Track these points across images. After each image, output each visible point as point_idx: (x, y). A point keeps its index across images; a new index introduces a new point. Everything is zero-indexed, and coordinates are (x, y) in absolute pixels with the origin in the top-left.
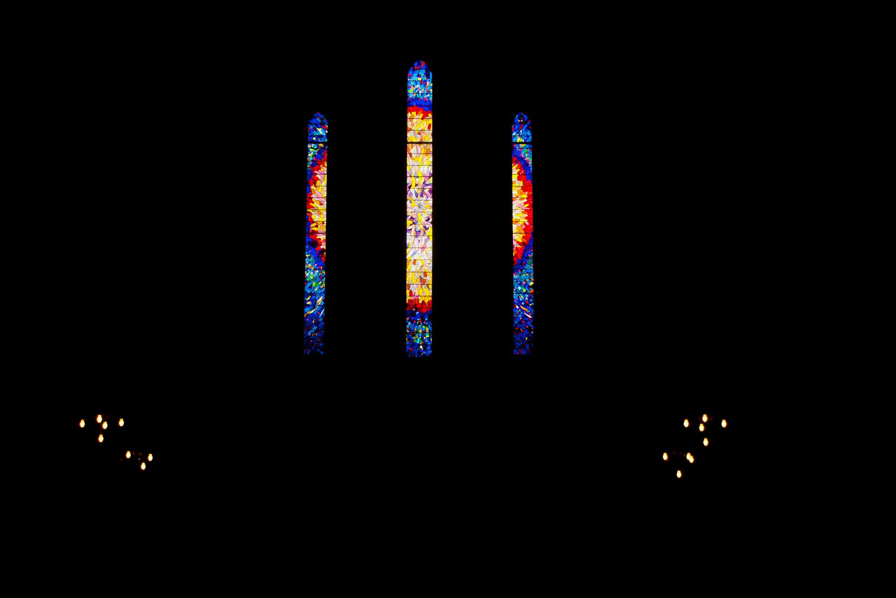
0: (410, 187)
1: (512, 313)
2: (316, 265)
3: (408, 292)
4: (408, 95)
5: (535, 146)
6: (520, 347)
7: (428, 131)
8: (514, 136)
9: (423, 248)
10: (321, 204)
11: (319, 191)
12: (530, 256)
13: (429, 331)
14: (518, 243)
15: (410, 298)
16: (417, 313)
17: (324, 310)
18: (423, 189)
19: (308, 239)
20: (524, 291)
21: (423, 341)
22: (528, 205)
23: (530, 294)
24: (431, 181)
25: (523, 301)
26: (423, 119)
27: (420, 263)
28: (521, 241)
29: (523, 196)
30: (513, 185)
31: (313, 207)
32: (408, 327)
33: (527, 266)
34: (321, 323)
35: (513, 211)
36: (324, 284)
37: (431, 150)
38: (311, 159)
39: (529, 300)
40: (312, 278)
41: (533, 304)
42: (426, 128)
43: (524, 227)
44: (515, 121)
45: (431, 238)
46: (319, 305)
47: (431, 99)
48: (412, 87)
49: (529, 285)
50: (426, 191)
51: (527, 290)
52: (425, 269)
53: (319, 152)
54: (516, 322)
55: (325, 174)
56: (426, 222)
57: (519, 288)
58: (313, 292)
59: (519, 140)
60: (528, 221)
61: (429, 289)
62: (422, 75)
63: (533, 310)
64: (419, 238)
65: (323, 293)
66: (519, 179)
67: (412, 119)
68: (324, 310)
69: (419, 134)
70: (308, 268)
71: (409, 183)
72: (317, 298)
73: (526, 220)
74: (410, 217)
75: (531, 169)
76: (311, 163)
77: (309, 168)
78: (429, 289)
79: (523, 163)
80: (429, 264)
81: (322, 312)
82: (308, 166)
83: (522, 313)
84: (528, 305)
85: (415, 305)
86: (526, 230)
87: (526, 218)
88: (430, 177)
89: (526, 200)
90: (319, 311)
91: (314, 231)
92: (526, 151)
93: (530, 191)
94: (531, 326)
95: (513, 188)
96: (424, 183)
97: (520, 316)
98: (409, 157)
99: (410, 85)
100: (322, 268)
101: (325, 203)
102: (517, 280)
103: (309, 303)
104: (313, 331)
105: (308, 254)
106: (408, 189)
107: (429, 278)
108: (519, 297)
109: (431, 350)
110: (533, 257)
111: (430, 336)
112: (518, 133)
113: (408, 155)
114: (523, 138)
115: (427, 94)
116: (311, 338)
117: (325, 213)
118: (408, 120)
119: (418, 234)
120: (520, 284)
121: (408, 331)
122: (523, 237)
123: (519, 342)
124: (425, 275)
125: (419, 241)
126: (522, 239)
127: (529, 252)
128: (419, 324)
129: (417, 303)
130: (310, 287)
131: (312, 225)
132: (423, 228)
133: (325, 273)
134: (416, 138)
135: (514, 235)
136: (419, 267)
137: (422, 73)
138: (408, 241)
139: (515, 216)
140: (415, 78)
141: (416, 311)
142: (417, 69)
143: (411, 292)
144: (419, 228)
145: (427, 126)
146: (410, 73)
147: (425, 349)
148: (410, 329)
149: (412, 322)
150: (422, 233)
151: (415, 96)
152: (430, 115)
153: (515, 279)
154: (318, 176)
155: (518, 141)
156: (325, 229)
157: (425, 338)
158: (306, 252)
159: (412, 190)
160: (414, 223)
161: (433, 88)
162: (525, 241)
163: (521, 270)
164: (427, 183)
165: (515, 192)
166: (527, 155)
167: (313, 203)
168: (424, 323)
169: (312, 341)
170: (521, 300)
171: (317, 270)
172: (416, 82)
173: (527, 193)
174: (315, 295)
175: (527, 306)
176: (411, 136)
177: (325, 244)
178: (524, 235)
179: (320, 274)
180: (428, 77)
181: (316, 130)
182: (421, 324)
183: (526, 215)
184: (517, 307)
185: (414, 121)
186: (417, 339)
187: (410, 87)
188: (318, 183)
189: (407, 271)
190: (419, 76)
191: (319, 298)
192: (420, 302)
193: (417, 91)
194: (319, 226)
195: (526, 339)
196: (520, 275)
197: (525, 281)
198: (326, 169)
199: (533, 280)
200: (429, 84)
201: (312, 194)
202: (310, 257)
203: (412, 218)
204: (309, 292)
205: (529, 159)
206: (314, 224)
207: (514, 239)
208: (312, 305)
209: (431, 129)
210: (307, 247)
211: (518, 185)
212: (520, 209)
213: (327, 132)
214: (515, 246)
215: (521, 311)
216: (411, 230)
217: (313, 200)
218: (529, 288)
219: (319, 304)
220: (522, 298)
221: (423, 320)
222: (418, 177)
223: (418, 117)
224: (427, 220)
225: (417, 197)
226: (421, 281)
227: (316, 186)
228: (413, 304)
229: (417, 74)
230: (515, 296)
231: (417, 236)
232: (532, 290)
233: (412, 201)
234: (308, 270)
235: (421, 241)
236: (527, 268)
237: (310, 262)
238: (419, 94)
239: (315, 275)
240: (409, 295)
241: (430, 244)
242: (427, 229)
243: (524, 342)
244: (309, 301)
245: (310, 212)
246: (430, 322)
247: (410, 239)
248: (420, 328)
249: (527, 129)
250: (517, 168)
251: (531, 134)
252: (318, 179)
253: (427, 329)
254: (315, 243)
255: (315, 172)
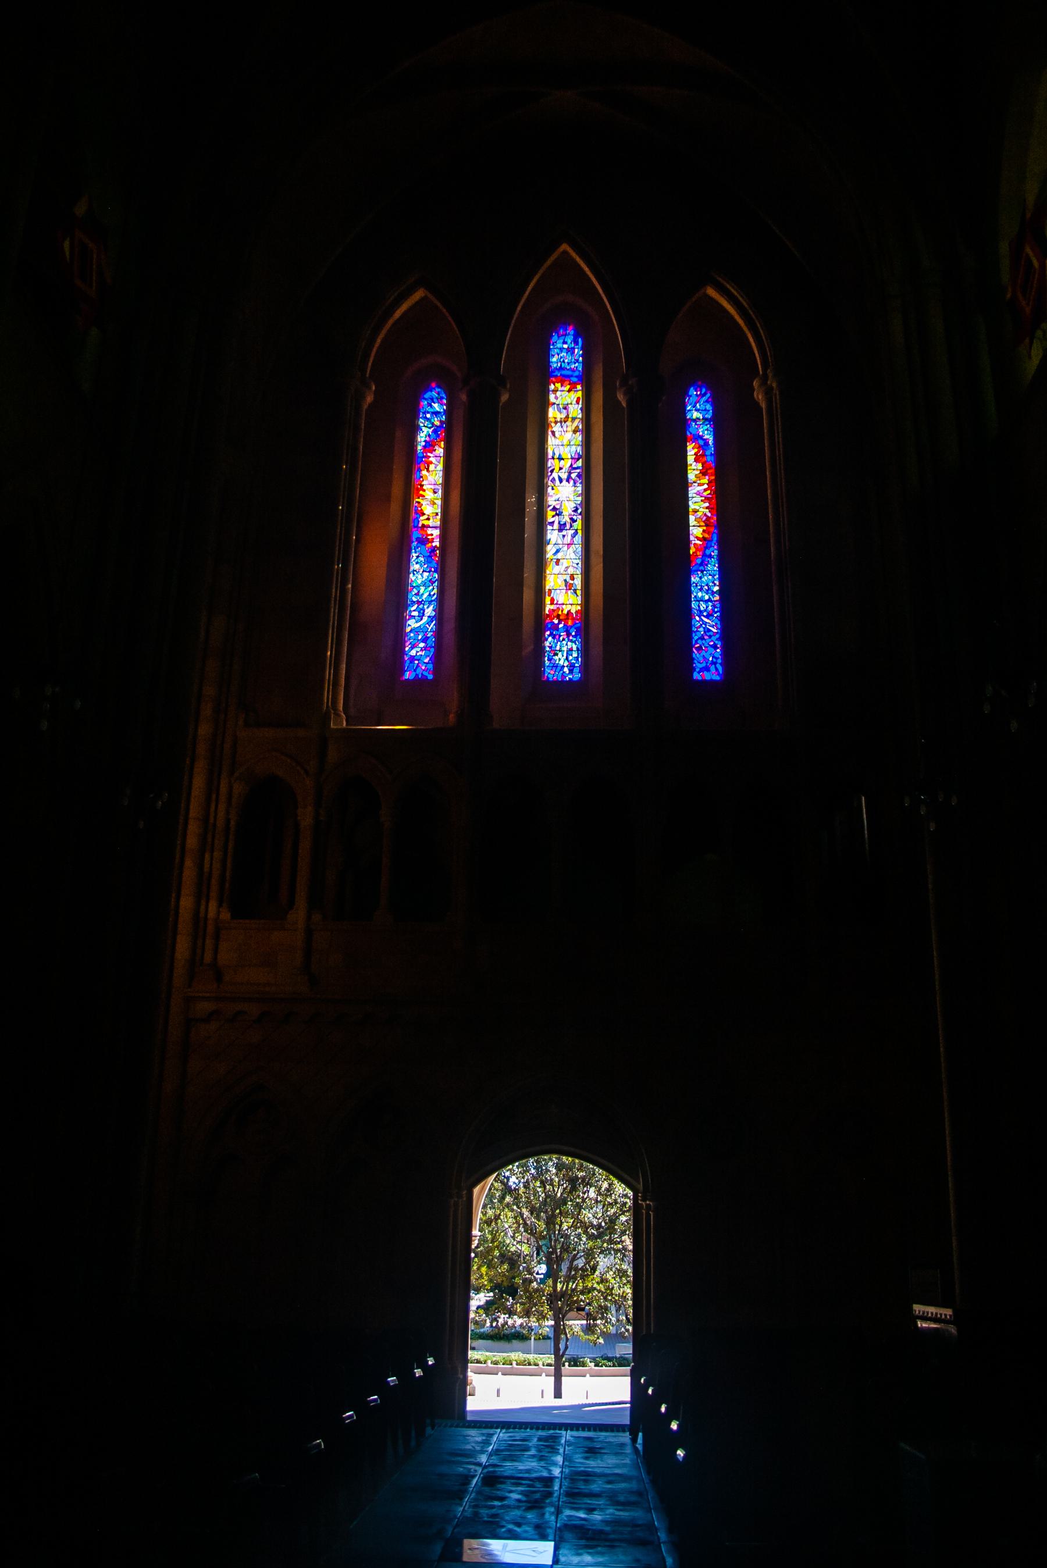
0: (552, 471)
1: (691, 626)
2: (426, 566)
3: (548, 600)
4: (551, 364)
5: (716, 422)
6: (702, 670)
7: (577, 405)
8: (689, 410)
9: (569, 545)
10: (435, 492)
11: (432, 476)
12: (713, 554)
13: (578, 649)
14: (698, 538)
15: (552, 607)
16: (561, 626)
17: (434, 622)
18: (570, 473)
19: (416, 535)
20: (707, 597)
21: (568, 661)
22: (709, 492)
23: (714, 601)
24: (579, 463)
25: (705, 610)
26: (569, 391)
27: (564, 563)
28: (701, 536)
29: (702, 481)
30: (689, 468)
31: (423, 496)
32: (547, 644)
33: (709, 567)
34: (430, 639)
35: (690, 499)
36: (435, 591)
37: (580, 427)
38: (423, 439)
39: (713, 610)
40: (419, 582)
41: (718, 614)
42: (574, 402)
43: (705, 518)
44: (690, 393)
45: (580, 532)
46: (429, 617)
47: (580, 369)
48: (556, 356)
49: (713, 591)
50: (573, 476)
51: (711, 596)
52: (571, 571)
53: (433, 432)
54: (696, 638)
55: (441, 457)
56: (573, 513)
57: (700, 594)
58: (420, 600)
59: (696, 415)
60: (709, 511)
61: (577, 596)
62: (569, 342)
63: (719, 623)
64: (564, 533)
65: (434, 601)
66: (696, 460)
67: (555, 391)
68: (434, 622)
69: (565, 408)
70: (414, 571)
71: (551, 467)
72: (425, 607)
73: (708, 510)
74: (551, 507)
75: (713, 449)
76: (423, 444)
77: (421, 450)
78: (577, 596)
79: (701, 442)
80: (577, 564)
81: (432, 624)
82: (419, 448)
83: (704, 626)
84: (713, 616)
85: (558, 616)
86: (707, 522)
87: (707, 508)
88: (578, 459)
89: (706, 486)
90: (427, 624)
91: (423, 525)
92: (705, 427)
93: (712, 475)
94: (716, 642)
95: (689, 472)
96: (571, 465)
97: (701, 629)
98: (551, 435)
99: (553, 354)
100: (433, 570)
101: (440, 491)
102: (696, 584)
103: (414, 614)
104: (419, 649)
105: (416, 552)
106: (549, 474)
107: (578, 582)
108: (699, 606)
109: (579, 672)
110: (718, 556)
111: (578, 654)
112: (694, 407)
113: (550, 433)
114: (700, 413)
115: (575, 363)
116: (415, 658)
117: (439, 502)
118: (551, 392)
119: (562, 527)
120: (701, 590)
121: (548, 649)
122: (704, 531)
123: (701, 663)
124: (572, 577)
125: (564, 536)
126: (701, 534)
127: (712, 549)
128: (564, 640)
129: (560, 613)
130: (417, 594)
131: (422, 518)
132: (569, 521)
133: (437, 577)
134: (561, 413)
135: (691, 528)
136: (563, 568)
137: (569, 339)
138: (549, 536)
139: (692, 506)
140: (559, 345)
141: (560, 623)
142: (562, 335)
143: (552, 600)
144: (564, 520)
145: (576, 399)
146: (555, 338)
147: (571, 671)
148: (550, 647)
149: (554, 638)
150: (568, 527)
151: (559, 365)
152: (579, 387)
153: (694, 583)
154: (431, 459)
155: (694, 417)
156: (439, 523)
157: (570, 658)
158: (413, 551)
159: (555, 475)
160: (556, 514)
161: (582, 356)
162: (706, 536)
163: (702, 571)
164: (575, 466)
165: (691, 476)
166: (706, 432)
167: (424, 491)
168: (571, 638)
169: (416, 662)
170: (702, 609)
171: (426, 572)
172: (561, 349)
173: (707, 477)
174: (424, 605)
175: (711, 618)
176: (552, 413)
177: (438, 540)
178: (705, 528)
179: (430, 578)
180: (576, 343)
181: (431, 406)
182: (566, 639)
183: (707, 504)
184: (697, 618)
185: (558, 394)
186: (560, 659)
187: (553, 356)
188: (432, 467)
189: (548, 572)
190: (565, 343)
191: (428, 607)
192: (565, 612)
193: (562, 360)
194: (431, 518)
195: (711, 659)
196: (701, 578)
197: (707, 585)
198: (442, 450)
199: (718, 584)
200: (578, 351)
201: (423, 481)
202: (418, 557)
203: (554, 509)
204: (414, 599)
205: (709, 437)
206: (425, 517)
207: (691, 533)
208: (419, 616)
209: (581, 403)
210: (415, 544)
211: (695, 468)
212: (698, 496)
213: (445, 407)
214: (693, 542)
215: (703, 624)
216: (553, 522)
217: (424, 487)
218: (712, 595)
219: (428, 615)
220: (703, 606)
221: (569, 634)
222: (563, 459)
223: (563, 388)
224: (576, 510)
225: (561, 481)
226: (566, 586)
227: (428, 470)
228: (555, 614)
229: (562, 341)
230: (694, 605)
231: (560, 530)
232: (717, 598)
233: (554, 487)
234: (415, 572)
235: (566, 537)
236: (709, 568)
237: (417, 563)
238: (564, 361)
239: (424, 579)
240: (549, 603)
241: (578, 539)
242: (576, 521)
243: (707, 663)
244: (414, 611)
245: (419, 503)
246: (578, 637)
247: (553, 535)
248: (565, 645)
249: (707, 401)
250: (693, 448)
251: (711, 408)
252: (431, 463)
253: (575, 648)
254: (424, 541)
255: (429, 454)
